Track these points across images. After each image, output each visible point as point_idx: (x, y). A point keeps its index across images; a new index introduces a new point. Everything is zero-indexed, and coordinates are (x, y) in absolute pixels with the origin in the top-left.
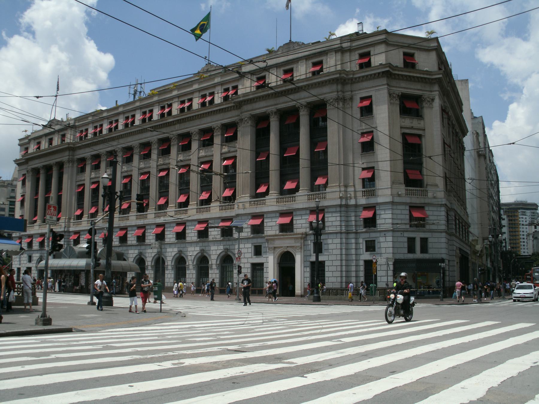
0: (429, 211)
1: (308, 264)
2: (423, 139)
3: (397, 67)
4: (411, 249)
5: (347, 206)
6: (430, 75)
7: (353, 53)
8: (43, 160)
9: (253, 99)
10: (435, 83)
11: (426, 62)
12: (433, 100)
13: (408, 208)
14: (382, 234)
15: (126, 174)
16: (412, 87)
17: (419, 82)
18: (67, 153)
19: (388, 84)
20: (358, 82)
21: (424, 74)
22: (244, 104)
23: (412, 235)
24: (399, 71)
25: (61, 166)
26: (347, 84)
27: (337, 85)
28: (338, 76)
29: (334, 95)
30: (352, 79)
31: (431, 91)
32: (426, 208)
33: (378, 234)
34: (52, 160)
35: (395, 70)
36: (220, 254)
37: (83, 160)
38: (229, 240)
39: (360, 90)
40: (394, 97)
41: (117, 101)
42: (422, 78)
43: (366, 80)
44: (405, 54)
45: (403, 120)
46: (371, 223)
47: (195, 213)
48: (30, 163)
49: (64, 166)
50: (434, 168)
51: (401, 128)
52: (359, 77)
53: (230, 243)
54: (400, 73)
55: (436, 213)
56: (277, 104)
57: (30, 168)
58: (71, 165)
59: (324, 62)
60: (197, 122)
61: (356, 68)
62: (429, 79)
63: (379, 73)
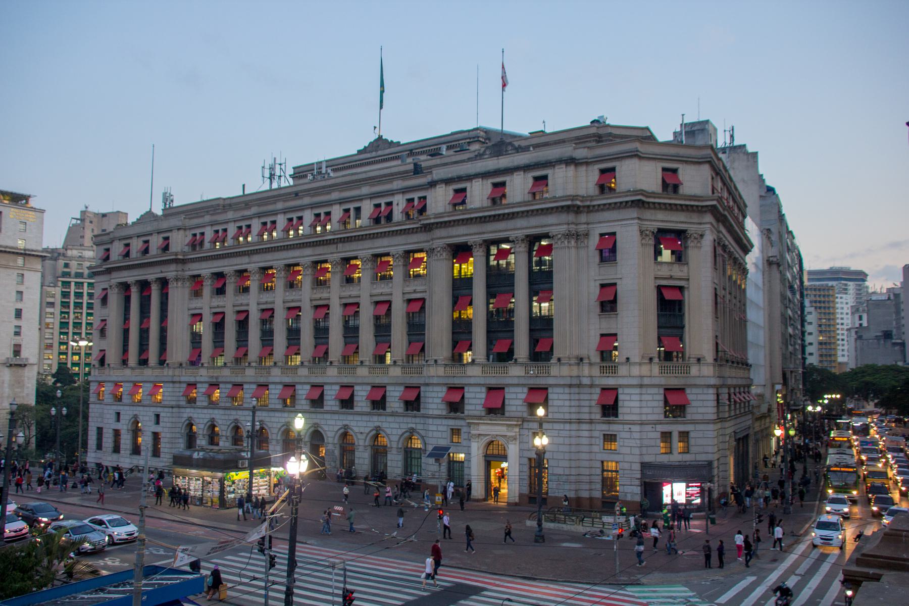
0: (691, 394)
1: (526, 461)
2: (686, 293)
3: (653, 193)
5: (579, 386)
6: (699, 201)
7: (590, 168)
9: (450, 222)
10: (705, 212)
11: (695, 181)
12: (702, 236)
13: (662, 391)
14: (627, 427)
15: (264, 307)
16: (674, 218)
17: (683, 210)
18: (173, 267)
19: (639, 219)
20: (597, 211)
21: (690, 200)
22: (437, 228)
23: (666, 428)
24: (655, 198)
25: (164, 283)
26: (581, 212)
28: (569, 203)
29: (563, 229)
30: (588, 207)
31: (700, 224)
32: (688, 391)
33: (620, 427)
34: (151, 275)
35: (650, 197)
36: (403, 434)
37: (197, 280)
38: (415, 417)
39: (600, 222)
40: (647, 235)
41: (244, 186)
42: (687, 206)
43: (608, 209)
44: (664, 169)
46: (610, 409)
48: (115, 275)
49: (170, 286)
50: (700, 330)
51: (656, 278)
52: (599, 205)
53: (418, 420)
54: (657, 200)
55: (700, 397)
56: (484, 233)
57: (114, 282)
58: (180, 284)
59: (550, 178)
60: (367, 244)
61: (593, 190)
62: (697, 206)
63: (627, 202)
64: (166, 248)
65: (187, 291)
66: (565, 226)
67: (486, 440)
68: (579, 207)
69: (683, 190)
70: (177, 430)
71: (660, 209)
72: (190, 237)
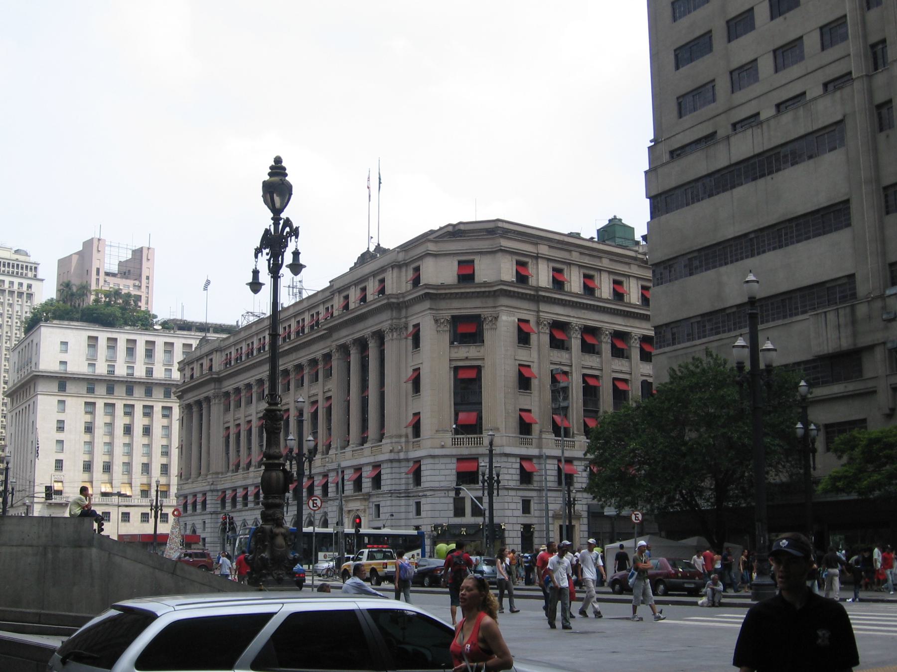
4: (459, 511)
8: (195, 393)
12: (496, 318)
13: (454, 460)
16: (469, 305)
17: (478, 297)
19: (430, 309)
24: (445, 289)
27: (392, 310)
31: (495, 307)
37: (227, 394)
44: (460, 262)
45: (456, 350)
47: (449, 442)
54: (447, 291)
61: (410, 286)
62: (489, 292)
64: (211, 368)
65: (222, 407)
66: (390, 322)
67: (352, 515)
68: (398, 304)
69: (477, 280)
70: (216, 535)
71: (455, 298)
72: (224, 357)
